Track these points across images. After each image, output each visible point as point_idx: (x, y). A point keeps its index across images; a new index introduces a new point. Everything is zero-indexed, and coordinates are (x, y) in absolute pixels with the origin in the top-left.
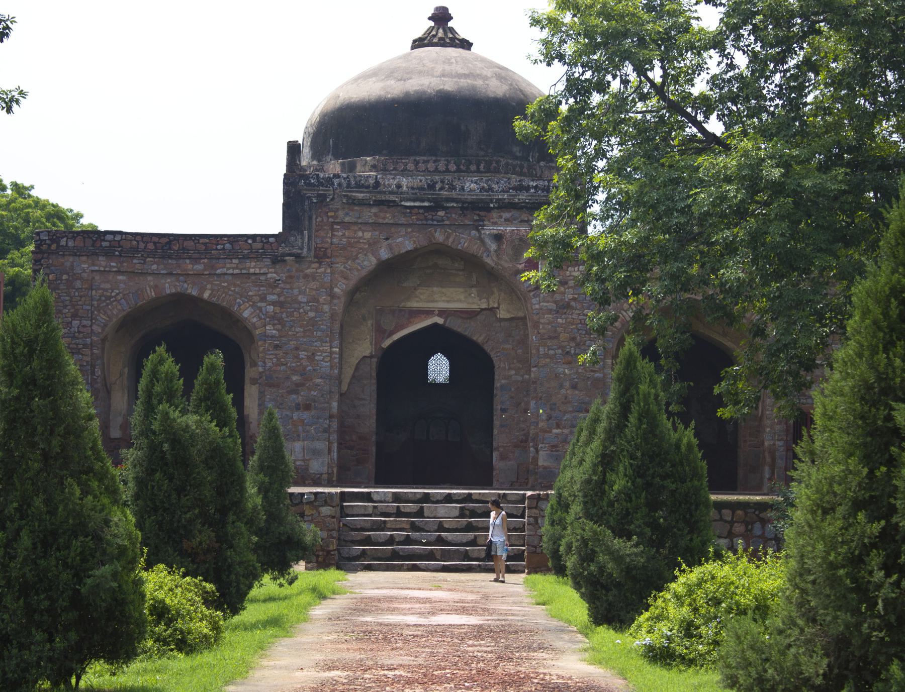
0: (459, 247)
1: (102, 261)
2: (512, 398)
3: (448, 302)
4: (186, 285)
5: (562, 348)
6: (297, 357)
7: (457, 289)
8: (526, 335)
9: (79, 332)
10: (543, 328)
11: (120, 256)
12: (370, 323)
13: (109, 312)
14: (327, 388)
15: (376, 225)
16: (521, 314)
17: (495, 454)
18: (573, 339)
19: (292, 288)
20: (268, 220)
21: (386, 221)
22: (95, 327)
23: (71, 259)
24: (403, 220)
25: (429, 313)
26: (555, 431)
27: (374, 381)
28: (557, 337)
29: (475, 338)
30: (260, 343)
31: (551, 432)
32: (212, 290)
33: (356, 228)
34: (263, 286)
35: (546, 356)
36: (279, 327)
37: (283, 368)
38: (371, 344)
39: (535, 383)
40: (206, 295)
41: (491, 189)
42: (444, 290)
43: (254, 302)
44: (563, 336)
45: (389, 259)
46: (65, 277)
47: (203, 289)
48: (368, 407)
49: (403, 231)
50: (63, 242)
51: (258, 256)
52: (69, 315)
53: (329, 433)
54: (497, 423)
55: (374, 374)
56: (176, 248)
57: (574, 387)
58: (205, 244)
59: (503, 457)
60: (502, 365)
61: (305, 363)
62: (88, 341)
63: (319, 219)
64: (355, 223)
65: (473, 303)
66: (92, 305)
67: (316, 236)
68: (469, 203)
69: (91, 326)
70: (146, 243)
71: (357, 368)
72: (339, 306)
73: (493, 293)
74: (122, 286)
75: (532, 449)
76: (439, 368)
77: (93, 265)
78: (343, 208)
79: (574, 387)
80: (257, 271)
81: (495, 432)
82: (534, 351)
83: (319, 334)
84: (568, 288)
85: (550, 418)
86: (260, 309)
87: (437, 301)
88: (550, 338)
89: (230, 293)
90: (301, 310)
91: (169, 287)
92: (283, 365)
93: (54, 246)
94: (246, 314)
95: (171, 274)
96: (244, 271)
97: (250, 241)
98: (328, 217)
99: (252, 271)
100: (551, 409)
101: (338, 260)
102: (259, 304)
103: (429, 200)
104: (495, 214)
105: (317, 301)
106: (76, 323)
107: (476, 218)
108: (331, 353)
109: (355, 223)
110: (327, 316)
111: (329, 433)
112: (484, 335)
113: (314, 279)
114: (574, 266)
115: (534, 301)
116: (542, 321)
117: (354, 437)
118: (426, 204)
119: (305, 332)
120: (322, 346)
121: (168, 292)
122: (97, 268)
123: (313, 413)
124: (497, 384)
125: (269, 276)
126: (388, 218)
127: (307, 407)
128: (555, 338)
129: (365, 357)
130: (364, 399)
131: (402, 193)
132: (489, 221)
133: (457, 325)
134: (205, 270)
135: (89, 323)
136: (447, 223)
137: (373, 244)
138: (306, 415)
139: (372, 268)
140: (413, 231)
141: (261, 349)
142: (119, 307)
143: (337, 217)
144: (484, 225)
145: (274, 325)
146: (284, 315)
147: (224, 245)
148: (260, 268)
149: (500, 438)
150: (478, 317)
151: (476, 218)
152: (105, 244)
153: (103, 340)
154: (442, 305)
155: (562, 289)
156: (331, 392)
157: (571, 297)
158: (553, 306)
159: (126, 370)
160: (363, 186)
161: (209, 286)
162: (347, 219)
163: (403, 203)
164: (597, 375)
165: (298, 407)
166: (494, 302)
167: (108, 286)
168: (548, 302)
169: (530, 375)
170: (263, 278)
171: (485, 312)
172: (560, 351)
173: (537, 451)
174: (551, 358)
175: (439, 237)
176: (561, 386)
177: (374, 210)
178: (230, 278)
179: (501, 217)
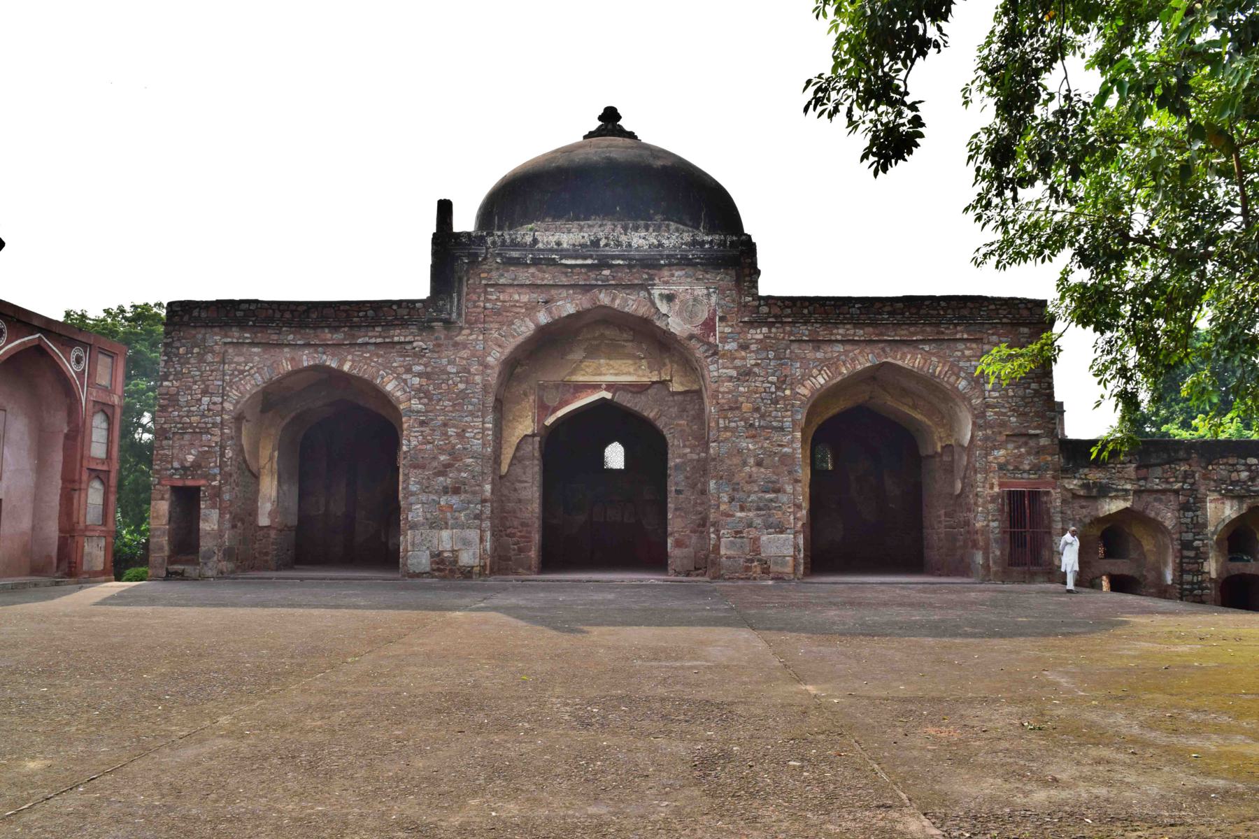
0: (626, 310)
1: (235, 334)
2: (687, 478)
3: (616, 375)
5: (746, 420)
6: (446, 434)
8: (702, 410)
9: (209, 410)
11: (254, 326)
12: (532, 398)
13: (242, 388)
14: (478, 469)
15: (534, 287)
16: (695, 387)
17: (670, 541)
18: (757, 410)
20: (414, 283)
21: (545, 282)
22: (226, 405)
23: (203, 331)
24: (565, 281)
25: (596, 387)
26: (739, 514)
27: (536, 462)
30: (404, 419)
32: (353, 361)
33: (511, 290)
35: (726, 428)
36: (426, 401)
37: (429, 447)
39: (714, 460)
40: (346, 368)
41: (660, 245)
42: (611, 362)
44: (746, 406)
45: (548, 325)
47: (342, 362)
48: (530, 492)
49: (564, 294)
50: (195, 313)
51: (403, 324)
53: (482, 520)
54: (671, 506)
55: (537, 454)
56: (314, 316)
57: (759, 464)
58: (346, 311)
59: (679, 544)
60: (676, 443)
61: (454, 440)
62: (218, 419)
63: (471, 281)
64: (511, 285)
67: (467, 300)
70: (283, 312)
71: (518, 448)
72: (493, 377)
73: (664, 365)
74: (257, 358)
75: (713, 536)
76: (615, 456)
77: (226, 336)
78: (498, 269)
79: (759, 464)
80: (402, 339)
81: (670, 516)
82: (713, 424)
83: (470, 407)
85: (732, 499)
86: (405, 381)
88: (731, 409)
91: (307, 359)
93: (186, 318)
94: (389, 387)
95: (307, 345)
97: (395, 307)
98: (481, 279)
99: (396, 339)
100: (734, 490)
103: (591, 257)
104: (666, 273)
105: (469, 372)
106: (206, 400)
107: (645, 276)
109: (511, 285)
110: (478, 388)
111: (482, 520)
113: (465, 346)
114: (756, 328)
115: (712, 368)
116: (722, 390)
118: (589, 262)
119: (454, 405)
121: (305, 364)
122: (229, 340)
123: (463, 497)
124: (671, 464)
125: (415, 344)
126: (547, 278)
127: (456, 491)
128: (738, 408)
129: (526, 436)
131: (562, 250)
133: (626, 400)
134: (345, 339)
135: (220, 400)
138: (454, 500)
139: (528, 334)
141: (405, 426)
145: (420, 399)
146: (431, 388)
149: (675, 523)
151: (645, 276)
152: (239, 314)
153: (239, 419)
154: (610, 379)
155: (743, 353)
157: (753, 362)
158: (734, 373)
159: (276, 454)
160: (516, 245)
161: (350, 357)
162: (502, 281)
163: (564, 261)
165: (445, 491)
167: (242, 359)
169: (707, 452)
170: (408, 347)
173: (719, 538)
174: (734, 430)
175: (604, 298)
176: (745, 463)
177: (532, 270)
178: (372, 348)
179: (673, 275)
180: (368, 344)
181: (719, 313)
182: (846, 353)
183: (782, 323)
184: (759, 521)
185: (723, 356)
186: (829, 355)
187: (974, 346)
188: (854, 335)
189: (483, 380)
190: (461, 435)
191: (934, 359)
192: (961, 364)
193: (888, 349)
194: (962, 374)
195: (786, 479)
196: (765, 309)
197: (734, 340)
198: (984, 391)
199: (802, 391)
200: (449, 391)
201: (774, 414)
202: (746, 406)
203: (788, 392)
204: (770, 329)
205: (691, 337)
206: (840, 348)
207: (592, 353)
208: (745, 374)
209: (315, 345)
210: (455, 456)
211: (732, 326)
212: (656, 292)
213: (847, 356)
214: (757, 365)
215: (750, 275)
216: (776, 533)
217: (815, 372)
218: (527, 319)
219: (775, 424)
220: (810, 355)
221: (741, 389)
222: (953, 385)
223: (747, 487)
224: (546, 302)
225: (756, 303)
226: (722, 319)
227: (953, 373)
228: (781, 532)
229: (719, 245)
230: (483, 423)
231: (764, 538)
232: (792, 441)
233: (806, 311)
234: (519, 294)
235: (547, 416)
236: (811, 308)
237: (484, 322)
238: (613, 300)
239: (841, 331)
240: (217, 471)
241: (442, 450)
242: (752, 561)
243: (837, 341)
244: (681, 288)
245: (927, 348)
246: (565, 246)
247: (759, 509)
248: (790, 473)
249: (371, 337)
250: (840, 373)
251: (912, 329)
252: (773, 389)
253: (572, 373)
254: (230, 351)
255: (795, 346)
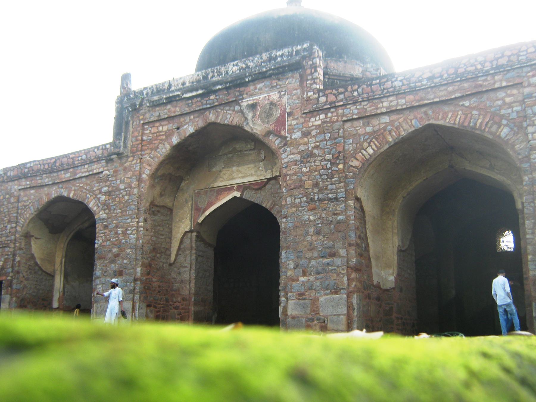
0: (226, 122)
3: (243, 177)
4: (62, 190)
5: (305, 195)
6: (116, 233)
7: (249, 166)
9: (10, 232)
10: (290, 179)
13: (25, 216)
15: (170, 118)
18: (316, 185)
19: (116, 180)
21: (177, 113)
24: (187, 110)
25: (230, 189)
26: (302, 279)
28: (301, 186)
29: (264, 206)
31: (297, 280)
32: (75, 190)
33: (157, 124)
34: (101, 182)
35: (293, 205)
36: (107, 211)
37: (108, 243)
38: (191, 221)
40: (71, 196)
41: (247, 67)
42: (240, 168)
43: (96, 195)
44: (308, 184)
45: (179, 144)
46: (7, 196)
49: (188, 119)
52: (6, 222)
57: (318, 233)
58: (72, 158)
61: (121, 237)
65: (261, 175)
66: (17, 213)
68: (230, 82)
69: (16, 227)
71: (181, 242)
77: (20, 185)
79: (318, 233)
83: (131, 212)
84: (311, 138)
85: (297, 266)
87: (235, 179)
89: (84, 191)
90: (121, 196)
91: (54, 192)
92: (109, 240)
95: (54, 184)
96: (91, 173)
98: (140, 120)
99: (95, 171)
100: (298, 257)
101: (146, 152)
102: (98, 196)
105: (130, 187)
106: (9, 226)
107: (237, 94)
108: (138, 227)
110: (135, 198)
112: (271, 201)
114: (315, 117)
116: (289, 173)
117: (179, 299)
118: (200, 92)
120: (132, 222)
125: (104, 173)
128: (301, 186)
129: (186, 232)
130: (186, 267)
132: (247, 94)
133: (251, 196)
134: (70, 177)
136: (217, 104)
137: (169, 134)
140: (194, 118)
142: (30, 212)
143: (145, 119)
144: (243, 99)
145: (105, 210)
147: (82, 156)
148: (99, 169)
150: (267, 187)
151: (237, 94)
153: (27, 236)
155: (306, 139)
156: (136, 259)
157: (313, 145)
159: (64, 260)
162: (152, 119)
163: (186, 96)
164: (340, 217)
166: (276, 171)
168: (294, 154)
170: (101, 176)
171: (272, 182)
172: (305, 199)
174: (298, 206)
175: (212, 117)
176: (307, 233)
177: (169, 107)
178: (84, 180)
179: (256, 88)
180: (81, 178)
181: (288, 110)
182: (392, 123)
183: (336, 107)
184: (317, 284)
185: (291, 145)
186: (375, 129)
187: (515, 91)
188: (397, 104)
189: (139, 191)
190: (124, 233)
191: (475, 112)
192: (503, 112)
193: (430, 112)
194: (504, 122)
195: (340, 244)
196: (323, 99)
197: (299, 130)
198: (526, 134)
199: (355, 163)
200: (120, 202)
201: (330, 187)
202: (308, 184)
203: (341, 166)
204: (326, 114)
205: (269, 133)
206: (386, 119)
207: (228, 164)
208: (308, 156)
209: (58, 183)
210: (122, 250)
211: (297, 119)
212: (244, 104)
213: (393, 125)
214: (317, 147)
215: (312, 74)
216: (332, 293)
217: (365, 144)
218: (166, 143)
219: (330, 196)
220: (361, 131)
221: (304, 170)
222: (493, 134)
223: (309, 255)
224: (178, 128)
225: (316, 96)
226: (290, 114)
227: (495, 123)
228: (336, 293)
229: (288, 56)
230: (138, 223)
231: (322, 299)
232: (346, 209)
233: (356, 94)
234: (162, 126)
235: (199, 216)
236: (360, 90)
237: (142, 150)
238: (217, 117)
239: (385, 104)
240: (10, 270)
241: (113, 244)
242: (312, 320)
243: (382, 114)
244: (262, 97)
245: (467, 103)
246: (187, 84)
247: (318, 273)
248: (344, 238)
249: (83, 173)
250: (387, 142)
251: (450, 89)
252: (329, 166)
253: (215, 181)
254: (22, 193)
255: (348, 125)
